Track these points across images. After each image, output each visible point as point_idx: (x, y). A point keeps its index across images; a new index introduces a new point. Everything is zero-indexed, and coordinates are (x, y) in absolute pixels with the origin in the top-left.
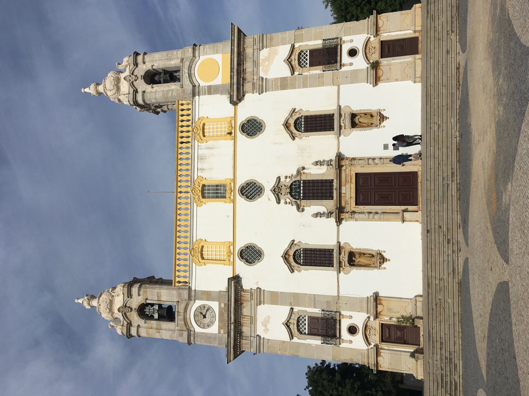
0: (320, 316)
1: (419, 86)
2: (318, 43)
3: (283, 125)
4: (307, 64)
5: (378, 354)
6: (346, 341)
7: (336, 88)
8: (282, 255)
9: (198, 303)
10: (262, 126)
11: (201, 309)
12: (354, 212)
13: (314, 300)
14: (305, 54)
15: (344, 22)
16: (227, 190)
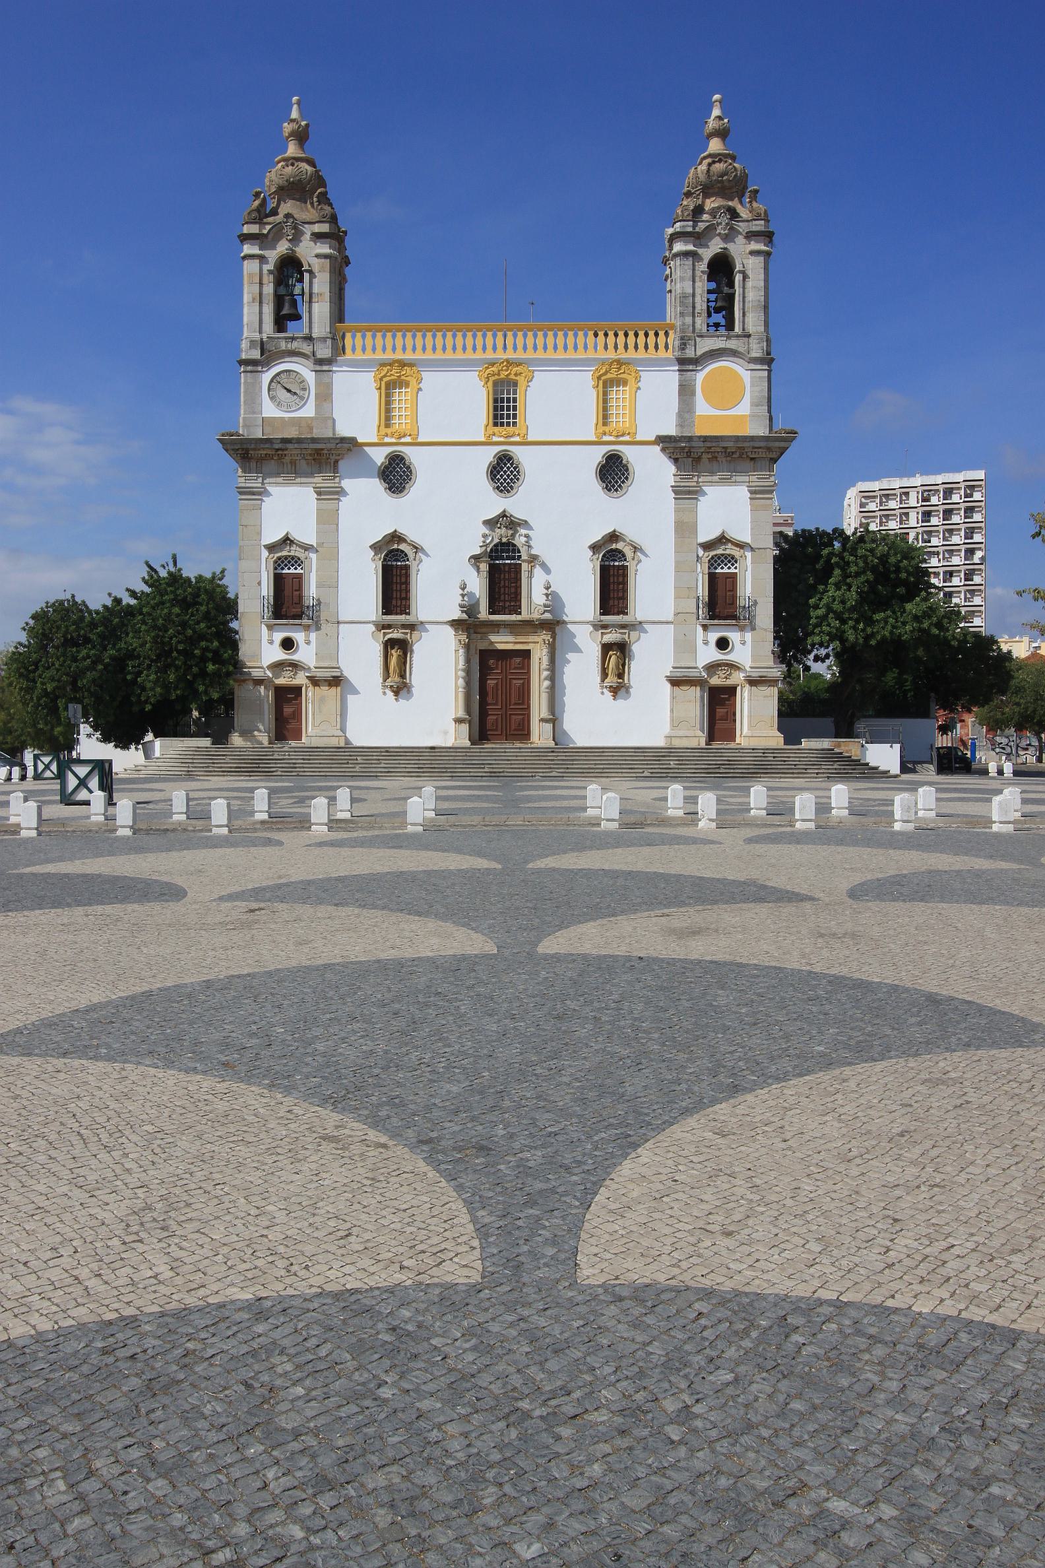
0: (305, 593)
1: (660, 742)
3: (614, 531)
5: (259, 682)
7: (671, 618)
9: (309, 376)
10: (616, 490)
11: (301, 383)
12: (467, 647)
13: (330, 583)
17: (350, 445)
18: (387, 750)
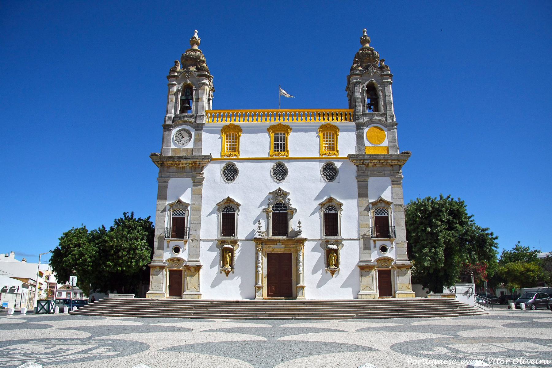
2: (392, 223)
4: (378, 214)
5: (162, 268)
6: (168, 244)
8: (230, 197)
14: (386, 212)
15: (407, 242)
16: (280, 152)
17: (208, 159)
18: (212, 302)
